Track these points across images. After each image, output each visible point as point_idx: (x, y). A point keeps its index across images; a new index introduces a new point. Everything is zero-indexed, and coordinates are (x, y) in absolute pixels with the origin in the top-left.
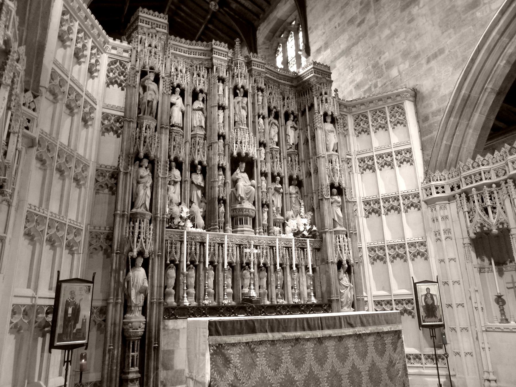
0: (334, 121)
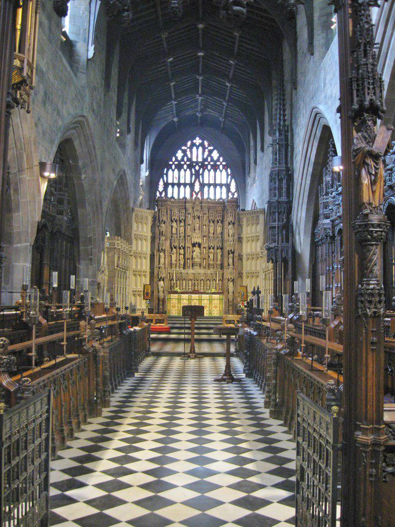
0: (233, 224)
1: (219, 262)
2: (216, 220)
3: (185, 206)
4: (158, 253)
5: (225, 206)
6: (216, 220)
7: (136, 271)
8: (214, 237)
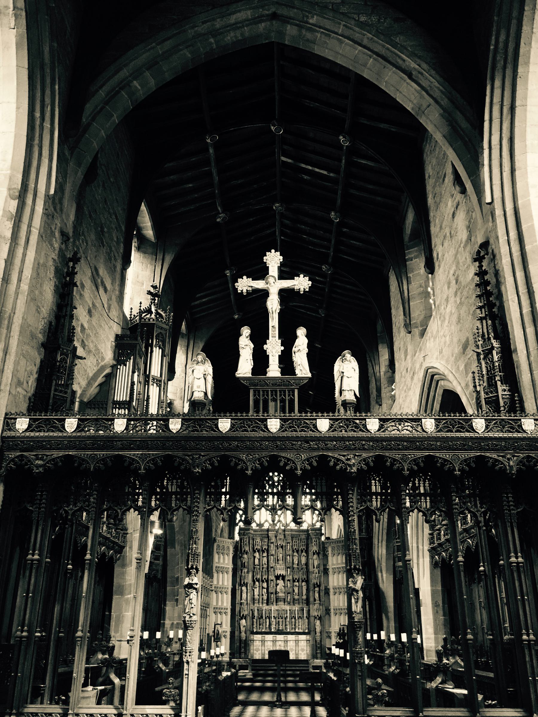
0: (318, 554)
1: (304, 597)
2: (300, 549)
3: (268, 534)
4: (240, 587)
5: (308, 535)
6: (300, 549)
7: (217, 608)
8: (298, 568)
